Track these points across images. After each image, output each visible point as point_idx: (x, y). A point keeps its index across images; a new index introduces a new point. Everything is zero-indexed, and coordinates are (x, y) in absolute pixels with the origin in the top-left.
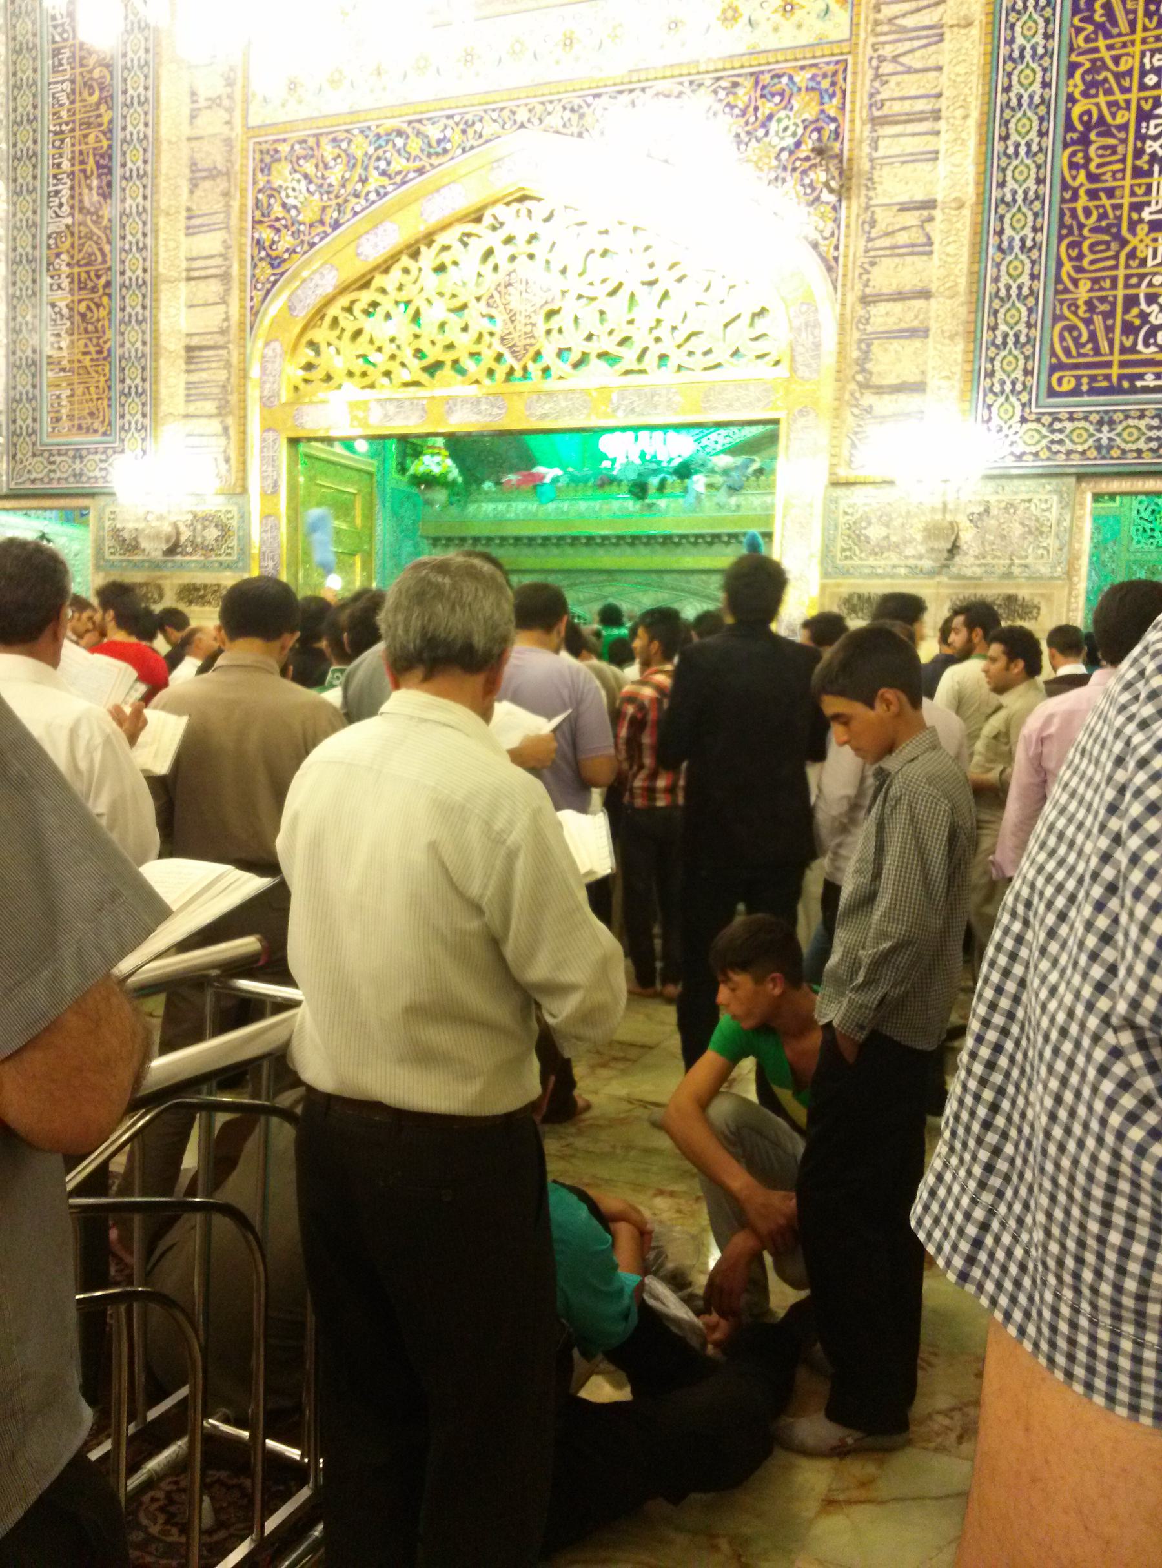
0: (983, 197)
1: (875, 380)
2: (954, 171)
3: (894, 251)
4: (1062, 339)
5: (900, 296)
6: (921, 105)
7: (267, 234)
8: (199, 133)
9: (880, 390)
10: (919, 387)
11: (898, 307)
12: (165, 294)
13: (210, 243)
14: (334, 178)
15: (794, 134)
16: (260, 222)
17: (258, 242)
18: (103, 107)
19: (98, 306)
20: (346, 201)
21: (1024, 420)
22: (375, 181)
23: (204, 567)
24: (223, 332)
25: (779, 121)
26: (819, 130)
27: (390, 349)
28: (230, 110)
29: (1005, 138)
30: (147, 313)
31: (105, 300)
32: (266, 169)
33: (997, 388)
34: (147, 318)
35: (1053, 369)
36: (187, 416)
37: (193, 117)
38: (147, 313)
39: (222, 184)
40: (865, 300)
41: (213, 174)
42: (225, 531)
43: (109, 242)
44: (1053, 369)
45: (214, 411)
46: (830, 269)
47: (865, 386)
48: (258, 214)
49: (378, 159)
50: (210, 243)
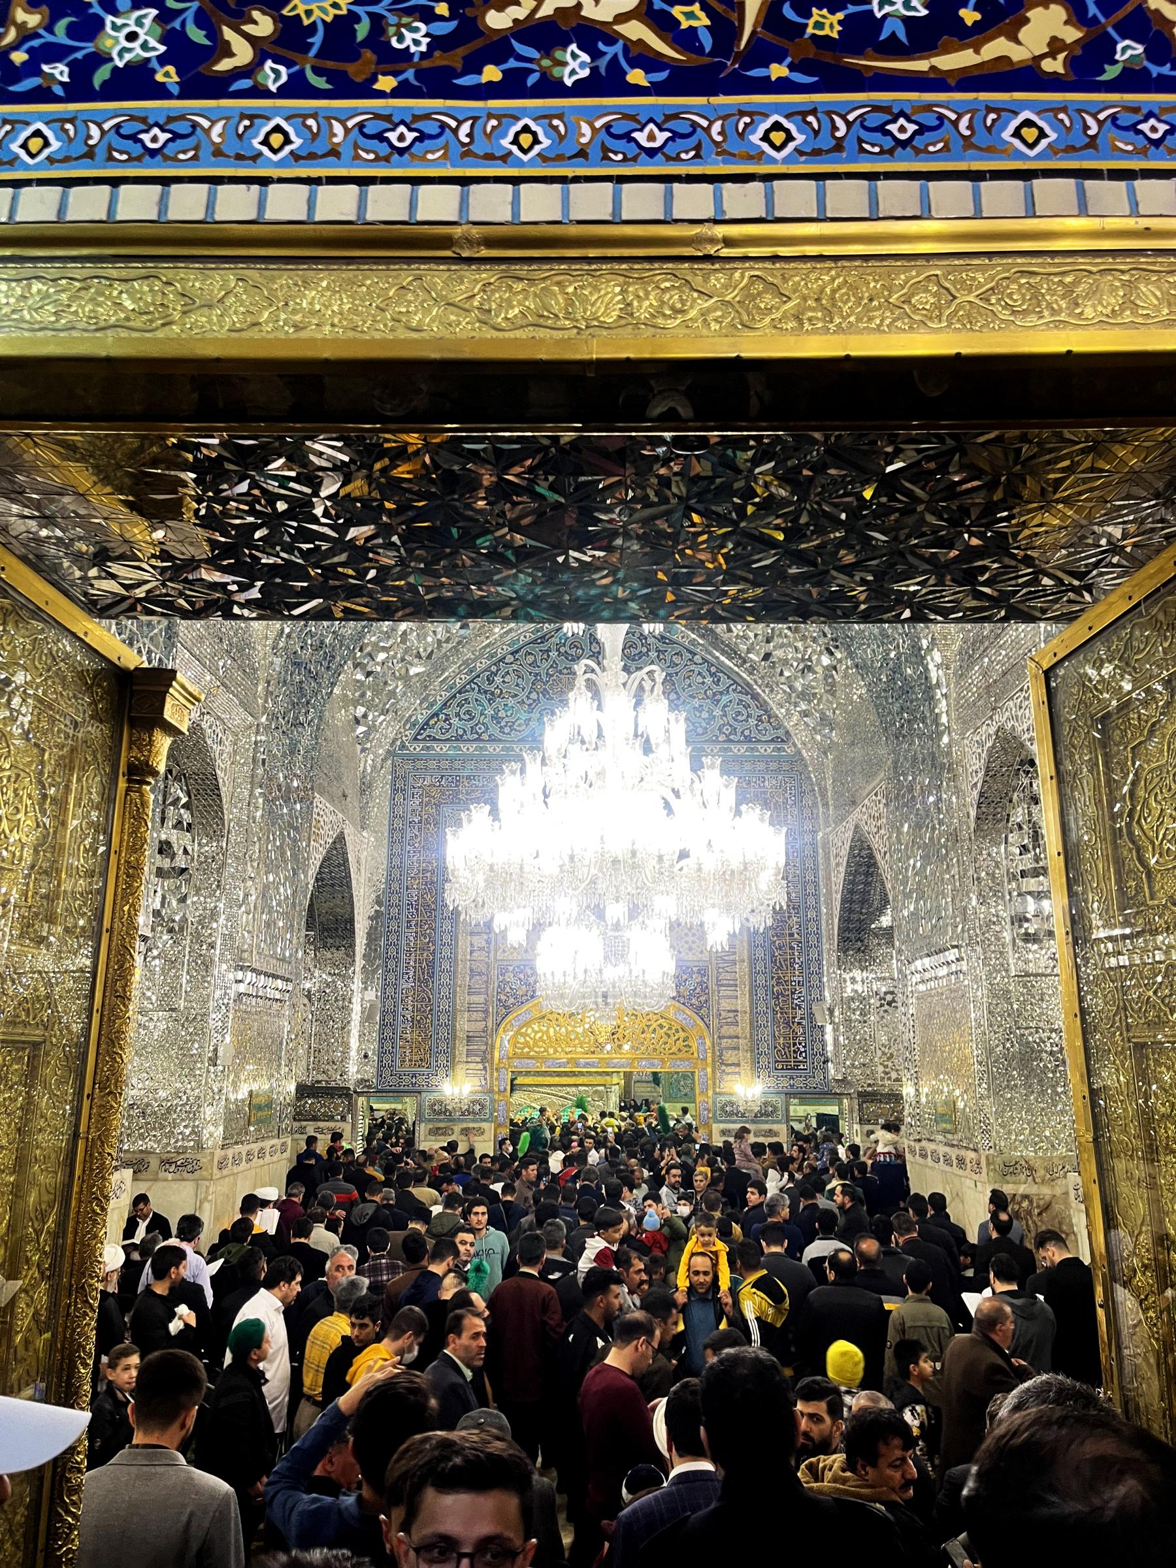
7: (503, 998)
10: (738, 1065)
23: (473, 1121)
41: (480, 974)
50: (480, 999)
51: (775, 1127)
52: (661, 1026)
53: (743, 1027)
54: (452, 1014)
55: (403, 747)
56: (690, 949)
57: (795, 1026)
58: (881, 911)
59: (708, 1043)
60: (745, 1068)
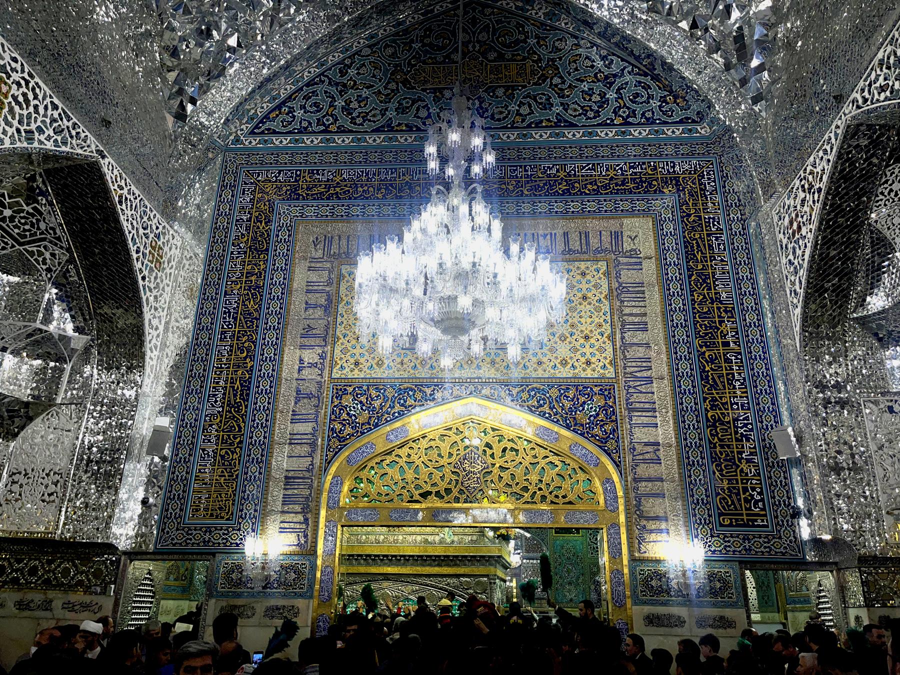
1: (645, 514)
2: (665, 431)
3: (645, 461)
4: (721, 503)
5: (649, 480)
6: (647, 406)
7: (338, 426)
8: (303, 377)
9: (649, 519)
11: (650, 484)
12: (276, 450)
13: (307, 428)
14: (377, 404)
15: (595, 411)
16: (334, 420)
17: (332, 429)
18: (248, 360)
19: (233, 453)
20: (382, 415)
21: (712, 536)
22: (398, 408)
24: (308, 470)
25: (588, 405)
26: (606, 410)
27: (401, 484)
28: (322, 370)
29: (684, 422)
30: (264, 458)
31: (238, 450)
32: (339, 397)
33: (698, 521)
34: (264, 462)
35: (720, 515)
36: (283, 512)
37: (299, 370)
38: (264, 458)
39: (314, 401)
40: (635, 480)
41: (309, 396)
42: (299, 573)
43: (243, 422)
44: (720, 515)
45: (300, 510)
46: (618, 466)
47: (641, 516)
48: (333, 417)
49: (400, 399)
50: (307, 428)
53: (669, 464)
54: (267, 448)
55: (237, 140)
56: (588, 363)
57: (744, 466)
59: (620, 493)
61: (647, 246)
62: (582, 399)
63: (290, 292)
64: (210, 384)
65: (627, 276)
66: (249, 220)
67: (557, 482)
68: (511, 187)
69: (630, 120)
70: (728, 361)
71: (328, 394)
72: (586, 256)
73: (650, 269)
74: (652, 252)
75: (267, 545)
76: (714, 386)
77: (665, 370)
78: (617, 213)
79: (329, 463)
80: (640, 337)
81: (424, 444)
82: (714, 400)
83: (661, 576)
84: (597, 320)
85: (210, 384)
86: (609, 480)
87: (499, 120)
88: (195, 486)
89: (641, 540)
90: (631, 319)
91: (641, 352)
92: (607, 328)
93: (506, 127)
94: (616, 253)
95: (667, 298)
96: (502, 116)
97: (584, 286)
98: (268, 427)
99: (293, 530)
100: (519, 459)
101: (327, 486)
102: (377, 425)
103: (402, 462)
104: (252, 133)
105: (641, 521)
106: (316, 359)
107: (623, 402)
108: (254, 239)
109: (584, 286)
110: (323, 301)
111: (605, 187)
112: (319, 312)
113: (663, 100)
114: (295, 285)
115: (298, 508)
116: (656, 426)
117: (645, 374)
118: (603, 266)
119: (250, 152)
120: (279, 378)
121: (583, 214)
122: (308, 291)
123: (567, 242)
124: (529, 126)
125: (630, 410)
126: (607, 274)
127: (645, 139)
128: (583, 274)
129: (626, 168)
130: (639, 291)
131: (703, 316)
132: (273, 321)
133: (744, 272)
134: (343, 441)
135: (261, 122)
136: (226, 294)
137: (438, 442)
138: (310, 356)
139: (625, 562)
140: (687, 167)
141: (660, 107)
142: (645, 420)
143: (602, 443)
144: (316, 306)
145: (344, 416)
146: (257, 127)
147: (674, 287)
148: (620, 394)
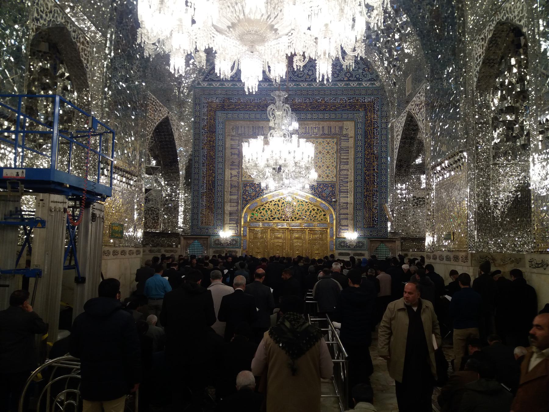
0: (354, 202)
2: (350, 199)
5: (344, 214)
7: (245, 197)
9: (342, 226)
10: (347, 226)
12: (226, 204)
13: (235, 197)
23: (233, 248)
37: (231, 177)
40: (339, 214)
41: (235, 187)
42: (236, 242)
50: (235, 197)
51: (363, 252)
52: (314, 210)
55: (199, 84)
57: (373, 210)
58: (417, 157)
59: (334, 217)
60: (351, 227)
61: (351, 133)
62: (325, 188)
63: (225, 149)
64: (201, 182)
65: (344, 144)
66: (207, 119)
67: (315, 215)
68: (304, 107)
69: (350, 78)
70: (374, 176)
71: (241, 186)
72: (329, 137)
73: (351, 141)
74: (353, 135)
75: (226, 234)
76: (368, 184)
77: (352, 179)
78: (341, 120)
79: (243, 208)
80: (346, 167)
81: (273, 203)
82: (367, 189)
83: (344, 242)
84: (332, 161)
85: (201, 182)
86: (332, 214)
87: (300, 77)
88: (200, 215)
89: (340, 232)
90: (343, 160)
91: (345, 172)
92: (335, 164)
93: (303, 81)
94: (339, 136)
95: (356, 153)
96: (301, 75)
97: (328, 148)
98: (223, 196)
99: (233, 229)
100: (303, 208)
101: (243, 215)
102: (258, 197)
103: (266, 208)
104: (204, 80)
105: (340, 226)
106: (236, 174)
107: (338, 190)
108: (210, 127)
109: (328, 148)
110: (237, 152)
111: (339, 108)
112: (236, 157)
113: (364, 70)
114: (227, 146)
115: (234, 222)
116: (348, 197)
117: (346, 180)
118: (335, 140)
119: (203, 89)
120: (224, 180)
121: (330, 120)
122: (232, 148)
123: (323, 131)
124: (312, 80)
125: (340, 192)
126: (337, 143)
127: (355, 87)
128: (328, 143)
129: (347, 100)
130: (347, 150)
131: (368, 159)
132: (220, 160)
133: (384, 143)
134: (247, 202)
135: (207, 75)
136: (202, 149)
137: (278, 202)
138: (234, 172)
139: (334, 238)
140: (369, 100)
141: (362, 73)
142: (344, 195)
143: (330, 203)
144: (234, 154)
145: (247, 193)
146: (206, 78)
147: (359, 149)
148: (337, 187)
